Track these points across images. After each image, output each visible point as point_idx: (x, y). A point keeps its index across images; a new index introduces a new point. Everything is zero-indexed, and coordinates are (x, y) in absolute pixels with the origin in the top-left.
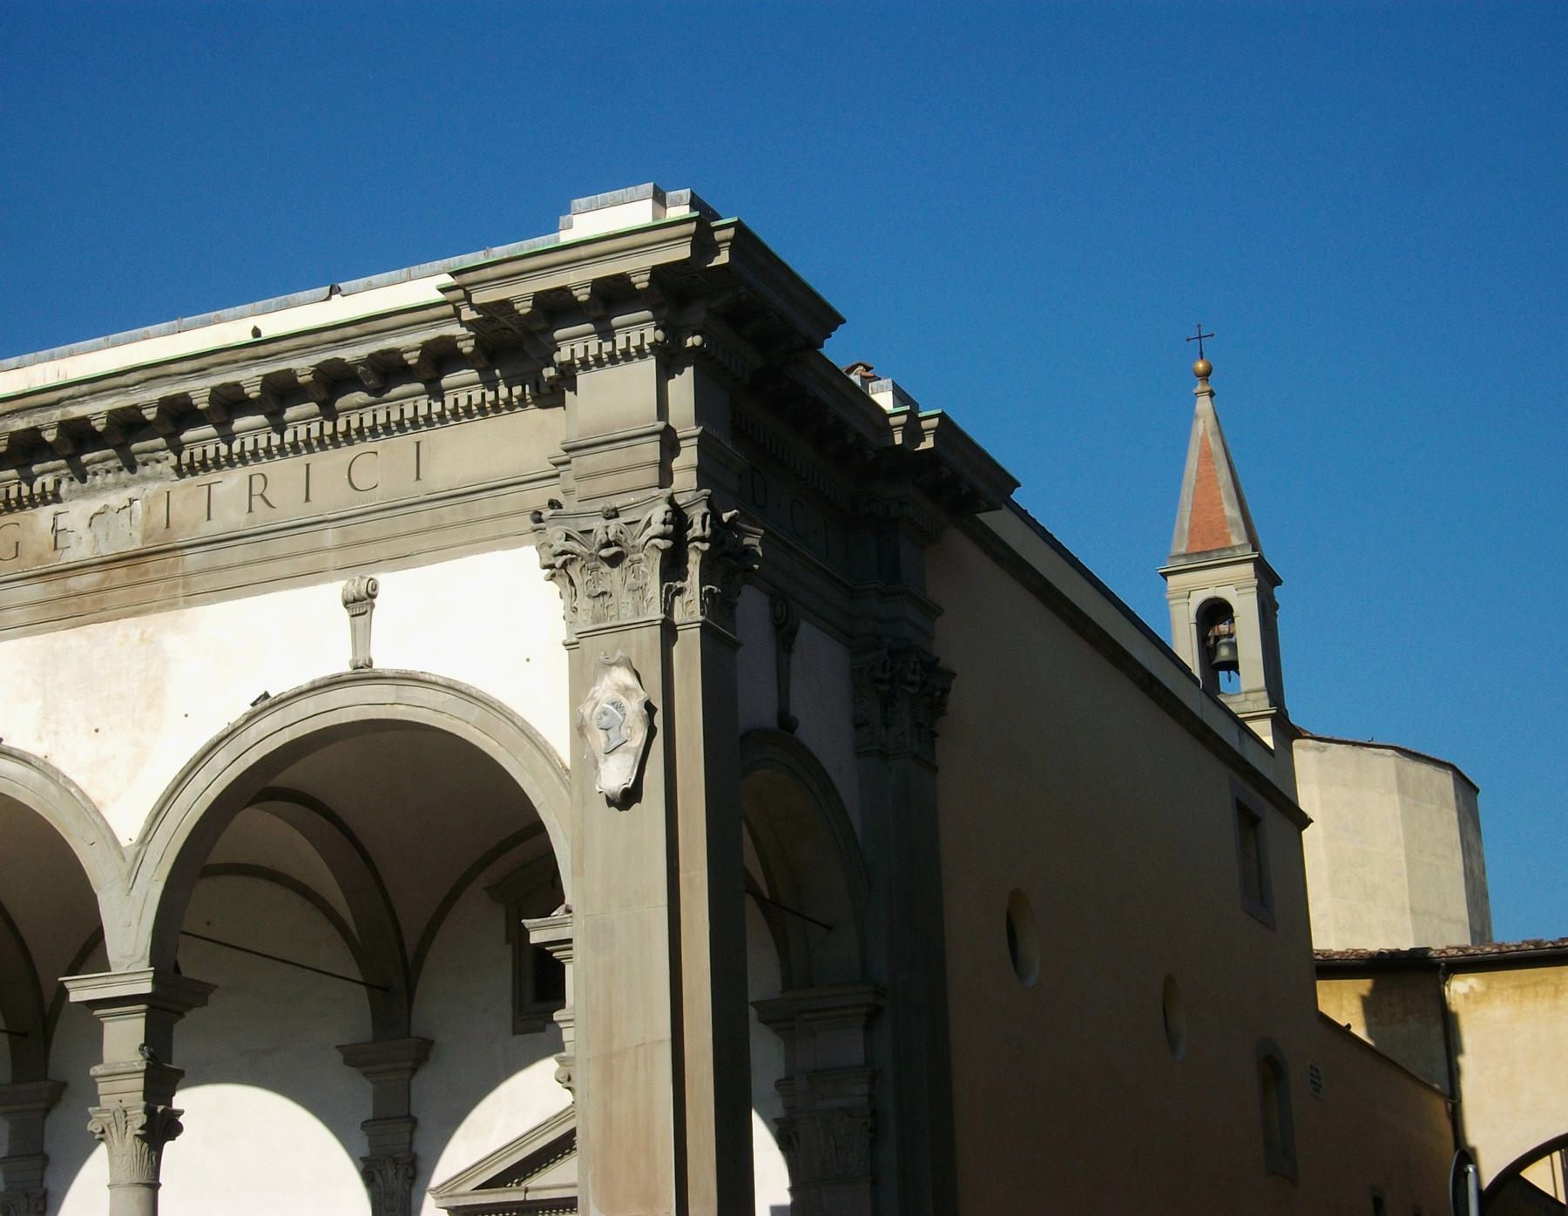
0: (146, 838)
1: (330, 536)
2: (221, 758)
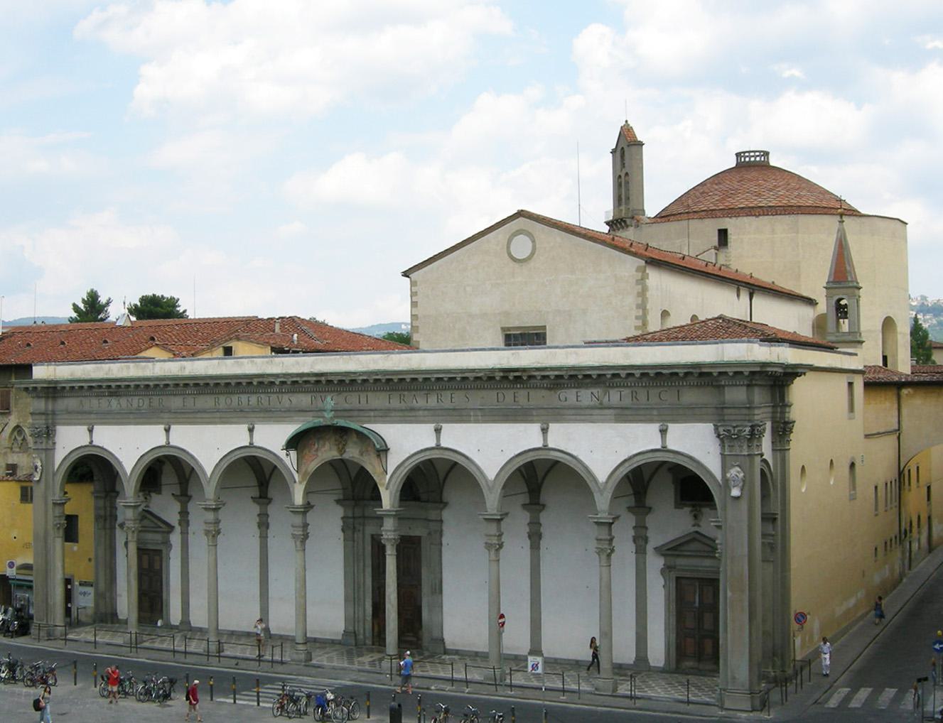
0: (607, 482)
1: (655, 412)
2: (627, 464)
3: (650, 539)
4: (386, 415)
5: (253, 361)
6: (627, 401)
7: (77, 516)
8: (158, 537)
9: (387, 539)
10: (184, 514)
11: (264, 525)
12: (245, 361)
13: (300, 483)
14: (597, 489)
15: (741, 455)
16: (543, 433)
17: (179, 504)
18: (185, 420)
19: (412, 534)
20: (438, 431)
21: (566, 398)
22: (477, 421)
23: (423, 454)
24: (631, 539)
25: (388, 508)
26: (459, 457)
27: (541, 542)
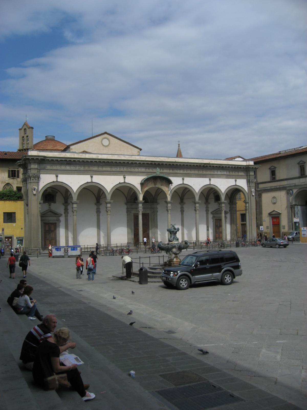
1: (234, 176)
4: (169, 174)
5: (125, 156)
7: (15, 213)
8: (55, 218)
9: (170, 209)
10: (66, 210)
11: (98, 212)
12: (122, 156)
17: (64, 206)
18: (99, 174)
20: (183, 179)
23: (179, 186)
24: (205, 211)
25: (170, 201)
26: (190, 187)
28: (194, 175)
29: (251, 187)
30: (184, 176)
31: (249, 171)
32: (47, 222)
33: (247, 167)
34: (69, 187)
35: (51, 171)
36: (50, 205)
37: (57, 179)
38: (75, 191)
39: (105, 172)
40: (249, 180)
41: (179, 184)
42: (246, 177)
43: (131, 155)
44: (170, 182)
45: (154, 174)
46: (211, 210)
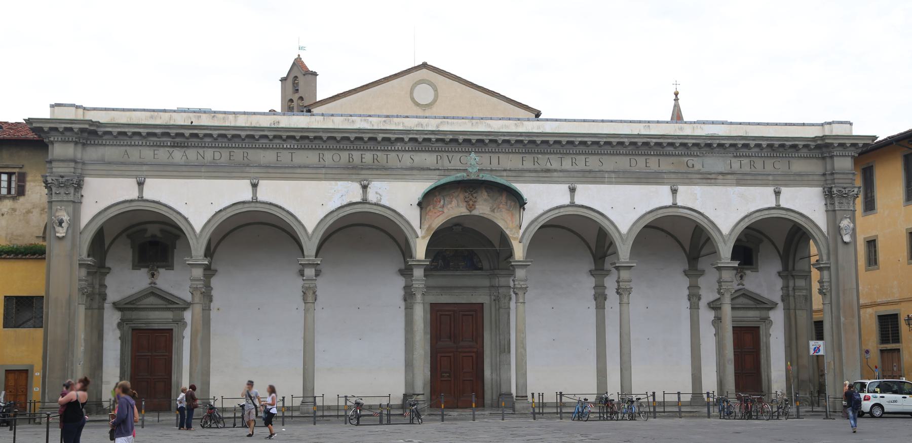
0: (730, 234)
1: (771, 178)
2: (747, 220)
3: (702, 297)
4: (521, 174)
6: (747, 168)
8: (169, 315)
13: (423, 238)
14: (721, 240)
15: (848, 210)
16: (673, 193)
19: (474, 300)
20: (572, 190)
21: (693, 165)
22: (610, 183)
23: (557, 211)
24: (686, 298)
25: (522, 259)
27: (606, 302)
28: (613, 175)
29: (837, 212)
30: (574, 178)
31: (832, 157)
32: (143, 326)
33: (819, 142)
34: (179, 217)
35: (123, 168)
36: (153, 275)
37: (141, 190)
38: (198, 228)
39: (299, 171)
40: (831, 188)
41: (555, 205)
42: (823, 178)
43: (387, 116)
44: (519, 201)
45: (459, 175)
46: (708, 295)
